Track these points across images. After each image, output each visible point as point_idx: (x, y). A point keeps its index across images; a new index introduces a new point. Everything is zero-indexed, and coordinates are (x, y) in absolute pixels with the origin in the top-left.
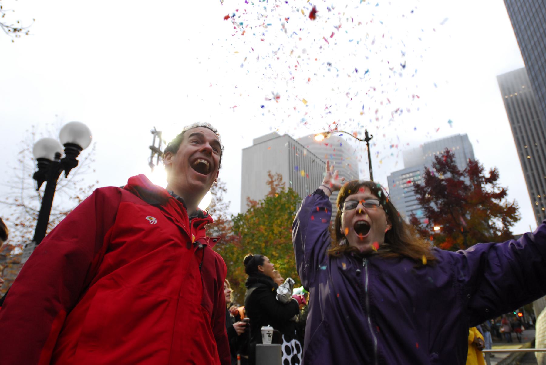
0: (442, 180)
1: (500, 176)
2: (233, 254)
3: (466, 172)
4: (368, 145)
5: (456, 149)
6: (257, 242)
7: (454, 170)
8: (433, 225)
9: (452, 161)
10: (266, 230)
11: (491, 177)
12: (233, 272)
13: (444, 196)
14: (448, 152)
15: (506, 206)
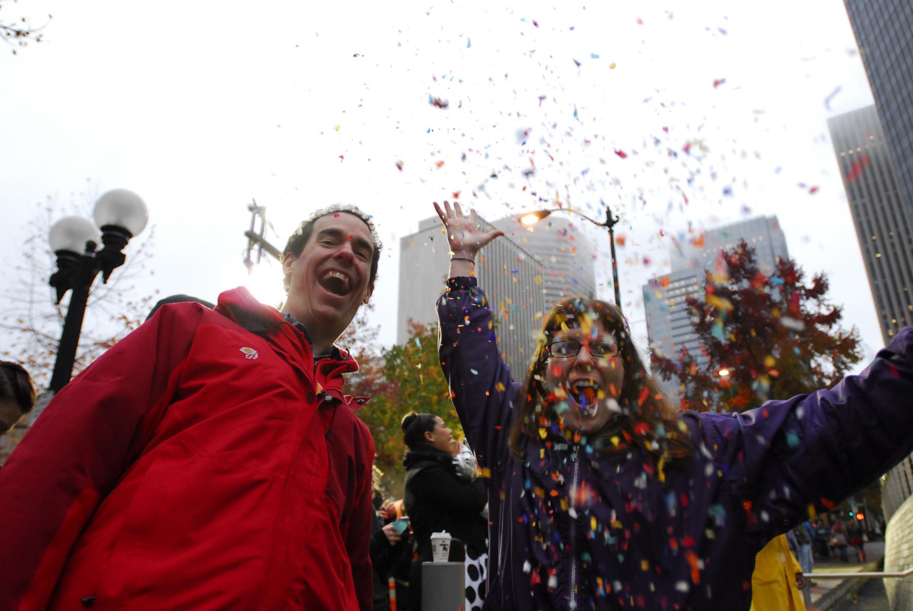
0: (734, 293)
1: (831, 287)
2: (384, 412)
4: (611, 232)
5: (758, 241)
6: (424, 394)
7: (753, 275)
8: (717, 367)
9: (751, 261)
11: (815, 289)
12: (383, 444)
14: (744, 246)
15: (840, 337)
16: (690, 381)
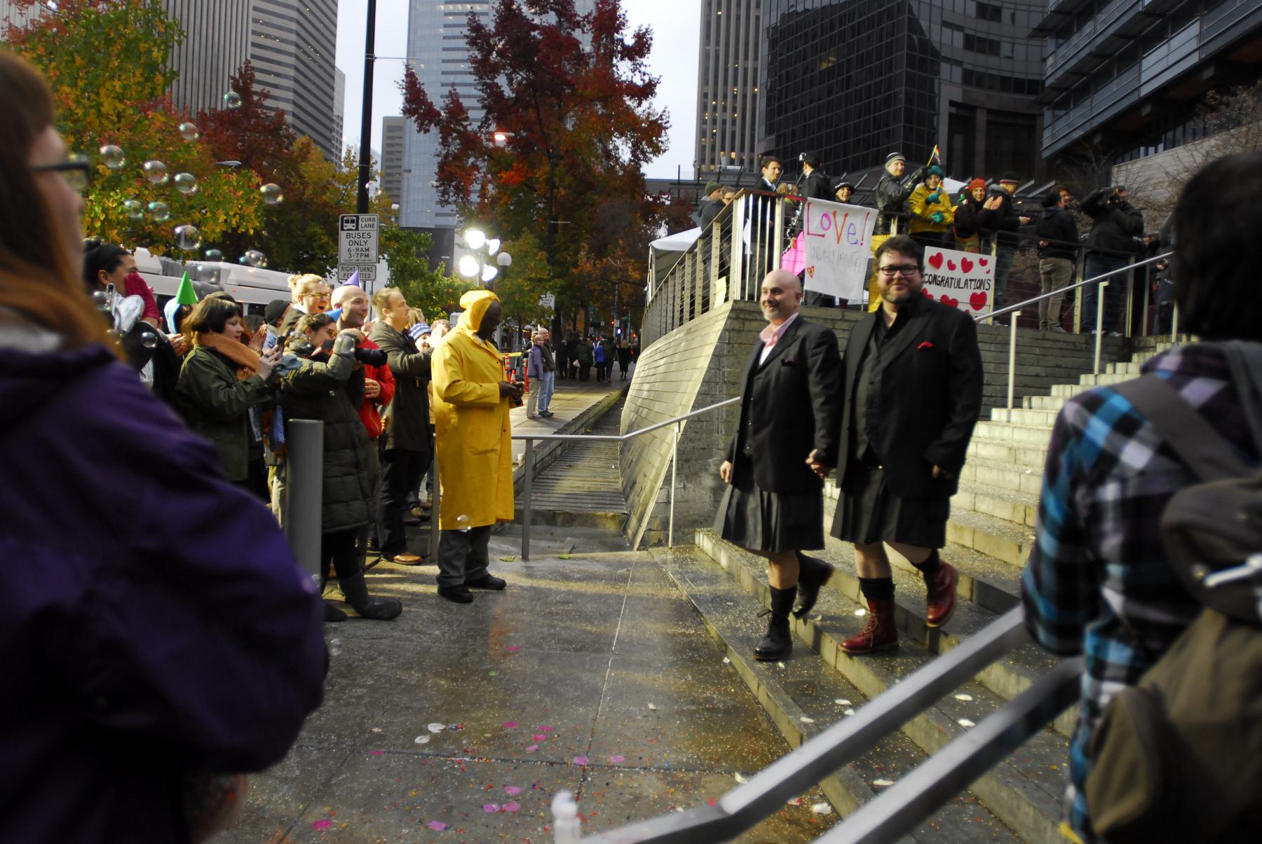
0: (535, 27)
1: (652, 49)
3: (589, 22)
8: (493, 127)
10: (77, 101)
13: (530, 67)
15: (648, 118)
16: (454, 139)
